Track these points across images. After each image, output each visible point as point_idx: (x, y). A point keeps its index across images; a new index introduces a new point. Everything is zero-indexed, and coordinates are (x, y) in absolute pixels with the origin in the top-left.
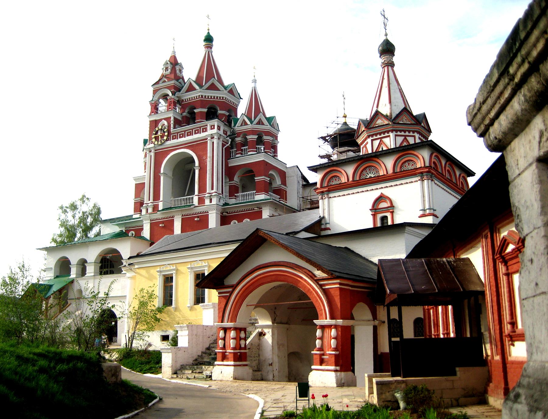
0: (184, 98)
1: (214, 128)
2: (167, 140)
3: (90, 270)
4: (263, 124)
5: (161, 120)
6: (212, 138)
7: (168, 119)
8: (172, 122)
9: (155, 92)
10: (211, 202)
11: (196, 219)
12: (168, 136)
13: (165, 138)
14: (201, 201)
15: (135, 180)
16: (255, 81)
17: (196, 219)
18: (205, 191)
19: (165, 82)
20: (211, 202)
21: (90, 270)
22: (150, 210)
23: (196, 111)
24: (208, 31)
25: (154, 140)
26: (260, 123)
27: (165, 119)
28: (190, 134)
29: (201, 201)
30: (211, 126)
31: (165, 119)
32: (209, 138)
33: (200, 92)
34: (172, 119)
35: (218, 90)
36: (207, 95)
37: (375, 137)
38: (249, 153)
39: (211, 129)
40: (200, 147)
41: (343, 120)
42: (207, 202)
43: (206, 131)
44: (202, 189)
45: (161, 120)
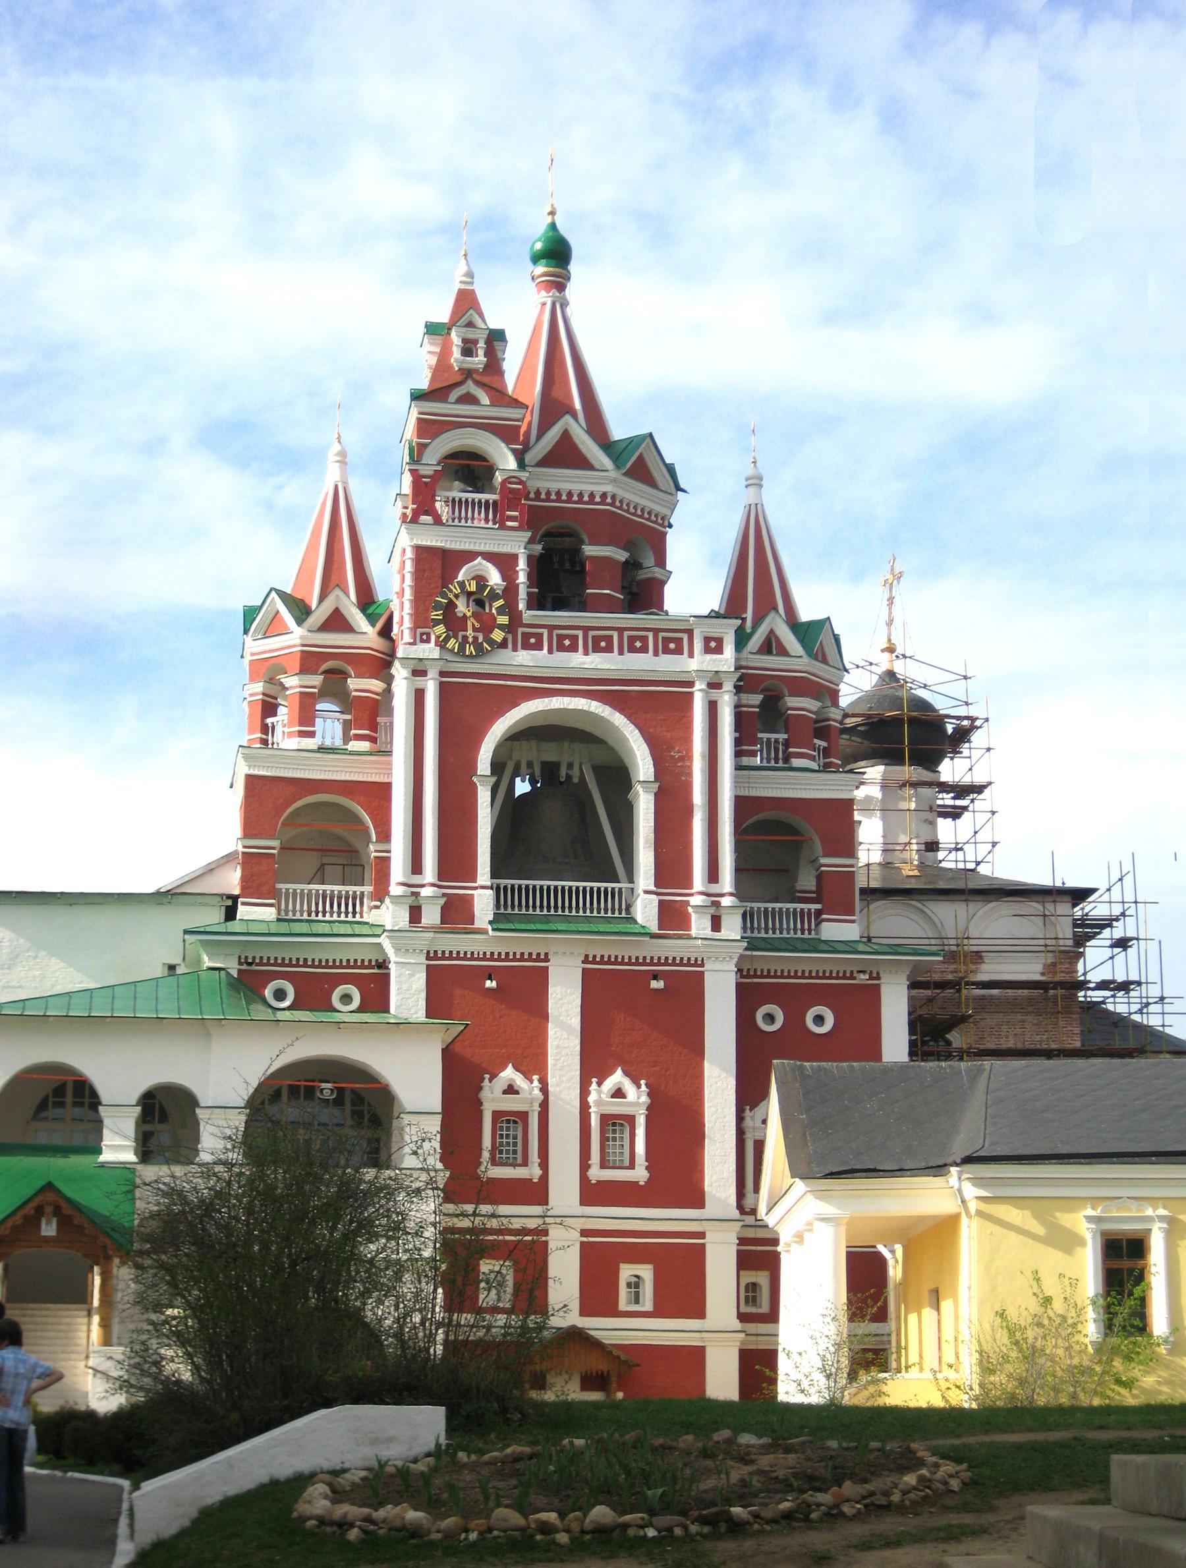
0: (533, 485)
1: (719, 650)
2: (503, 645)
4: (824, 661)
6: (714, 685)
8: (522, 578)
9: (428, 428)
10: (716, 924)
11: (654, 984)
12: (510, 628)
13: (498, 635)
14: (673, 917)
15: (246, 758)
17: (654, 984)
18: (685, 880)
19: (469, 399)
20: (716, 924)
22: (431, 915)
23: (590, 550)
24: (549, 219)
25: (440, 629)
26: (771, 645)
27: (490, 557)
28: (600, 645)
29: (673, 917)
30: (707, 640)
31: (490, 557)
32: (699, 685)
33: (614, 481)
34: (522, 564)
35: (652, 483)
36: (628, 496)
38: (796, 762)
39: (708, 650)
40: (660, 708)
41: (884, 663)
42: (699, 925)
43: (678, 651)
44: (673, 870)
45: (468, 556)
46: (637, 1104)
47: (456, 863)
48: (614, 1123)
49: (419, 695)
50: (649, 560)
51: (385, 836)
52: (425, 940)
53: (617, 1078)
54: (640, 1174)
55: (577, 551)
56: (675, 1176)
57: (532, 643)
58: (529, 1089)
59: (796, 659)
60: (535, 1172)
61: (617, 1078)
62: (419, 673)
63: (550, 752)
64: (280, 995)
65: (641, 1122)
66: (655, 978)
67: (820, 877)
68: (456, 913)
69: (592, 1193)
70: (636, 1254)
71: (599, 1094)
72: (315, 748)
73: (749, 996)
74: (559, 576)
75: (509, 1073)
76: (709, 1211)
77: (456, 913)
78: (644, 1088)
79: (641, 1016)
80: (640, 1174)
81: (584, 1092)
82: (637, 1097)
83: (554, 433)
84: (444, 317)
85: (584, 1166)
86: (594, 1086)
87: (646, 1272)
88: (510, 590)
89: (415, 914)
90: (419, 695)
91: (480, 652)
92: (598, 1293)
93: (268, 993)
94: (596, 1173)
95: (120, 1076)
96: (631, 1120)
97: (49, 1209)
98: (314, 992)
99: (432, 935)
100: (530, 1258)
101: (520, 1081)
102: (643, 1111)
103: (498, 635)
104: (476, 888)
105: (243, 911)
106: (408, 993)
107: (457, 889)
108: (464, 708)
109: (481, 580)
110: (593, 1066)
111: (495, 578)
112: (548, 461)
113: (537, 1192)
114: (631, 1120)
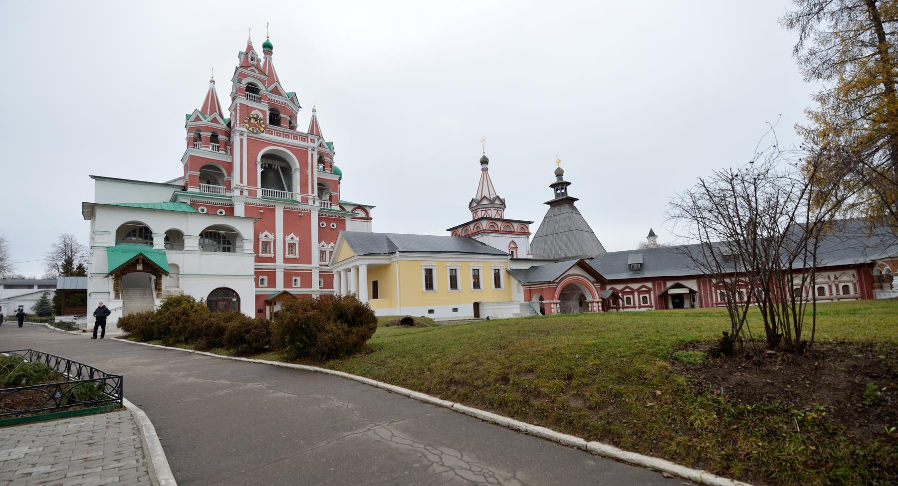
3: (192, 243)
5: (255, 109)
7: (264, 112)
12: (265, 128)
14: (305, 200)
16: (314, 110)
18: (307, 192)
19: (253, 71)
21: (192, 243)
22: (246, 193)
23: (282, 115)
28: (287, 136)
29: (305, 200)
34: (268, 113)
42: (311, 202)
45: (255, 109)
47: (252, 181)
48: (291, 246)
49: (241, 140)
50: (293, 122)
51: (230, 174)
52: (244, 199)
54: (297, 256)
55: (278, 115)
56: (306, 257)
57: (270, 133)
58: (271, 237)
59: (326, 150)
60: (272, 255)
61: (292, 235)
63: (270, 162)
64: (203, 210)
67: (331, 197)
68: (252, 194)
69: (286, 260)
70: (297, 274)
71: (288, 238)
72: (207, 152)
73: (320, 219)
74: (275, 119)
75: (266, 233)
76: (313, 265)
77: (252, 194)
79: (296, 221)
80: (297, 256)
82: (296, 240)
83: (273, 86)
84: (244, 51)
87: (299, 279)
88: (265, 119)
89: (242, 192)
90: (241, 140)
91: (258, 133)
92: (288, 282)
93: (199, 209)
94: (287, 256)
95: (159, 226)
97: (141, 261)
98: (212, 211)
100: (272, 275)
101: (269, 234)
103: (262, 129)
105: (190, 189)
106: (239, 210)
107: (252, 188)
108: (255, 145)
109: (258, 116)
110: (286, 232)
111: (261, 115)
112: (271, 92)
113: (273, 260)
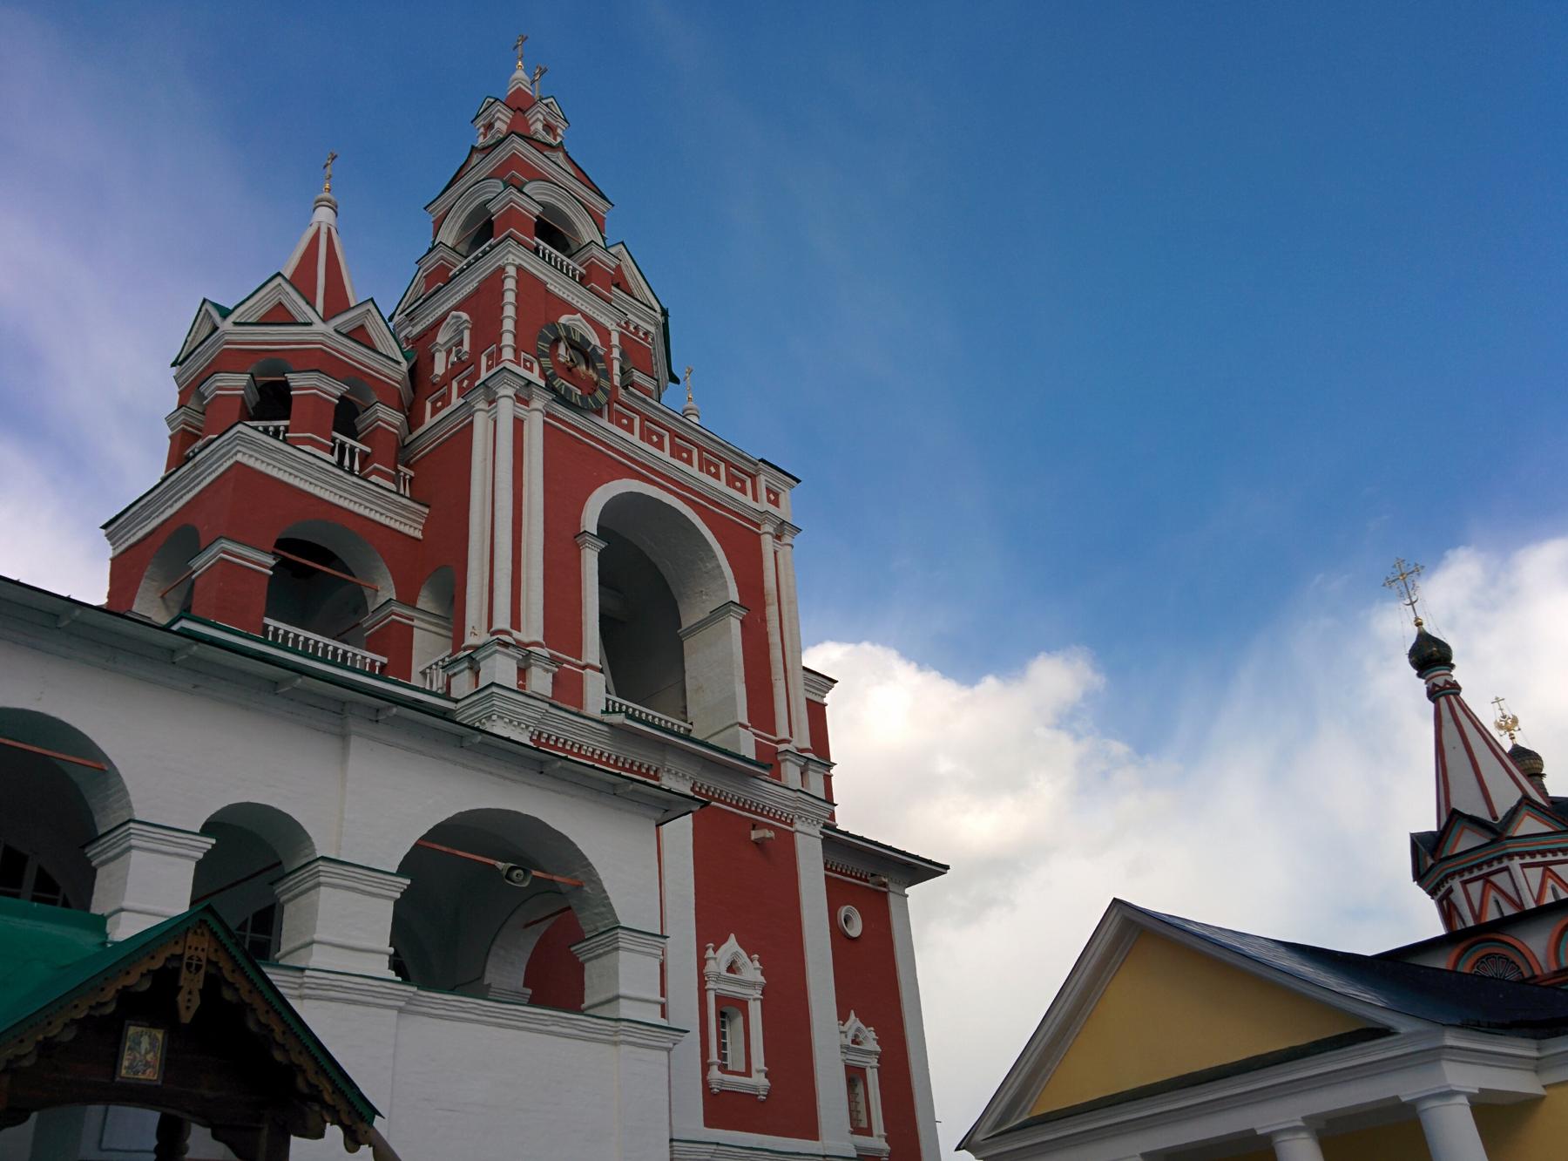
5: (574, 311)
37: (1528, 860)
45: (574, 311)
46: (753, 985)
49: (518, 423)
53: (732, 946)
54: (759, 1081)
61: (732, 946)
62: (522, 400)
65: (755, 1010)
66: (754, 827)
78: (757, 964)
81: (702, 962)
85: (706, 1067)
86: (710, 953)
96: (742, 1005)
99: (546, 706)
102: (757, 994)
104: (584, 668)
114: (742, 1005)
